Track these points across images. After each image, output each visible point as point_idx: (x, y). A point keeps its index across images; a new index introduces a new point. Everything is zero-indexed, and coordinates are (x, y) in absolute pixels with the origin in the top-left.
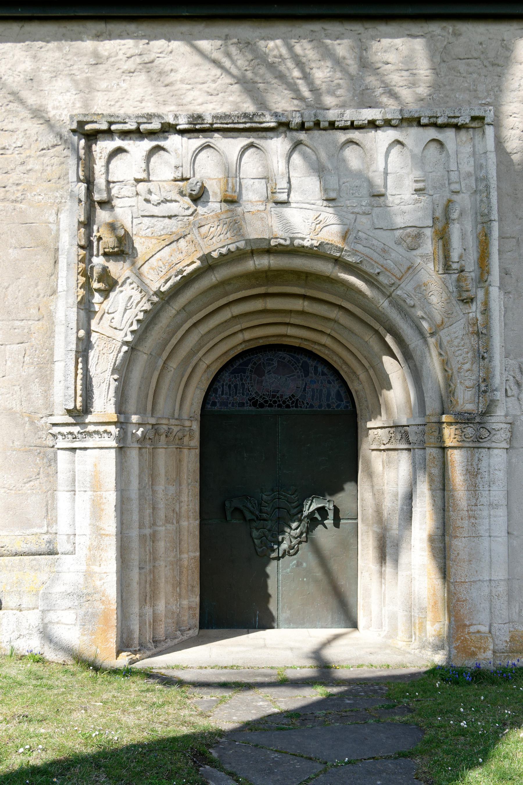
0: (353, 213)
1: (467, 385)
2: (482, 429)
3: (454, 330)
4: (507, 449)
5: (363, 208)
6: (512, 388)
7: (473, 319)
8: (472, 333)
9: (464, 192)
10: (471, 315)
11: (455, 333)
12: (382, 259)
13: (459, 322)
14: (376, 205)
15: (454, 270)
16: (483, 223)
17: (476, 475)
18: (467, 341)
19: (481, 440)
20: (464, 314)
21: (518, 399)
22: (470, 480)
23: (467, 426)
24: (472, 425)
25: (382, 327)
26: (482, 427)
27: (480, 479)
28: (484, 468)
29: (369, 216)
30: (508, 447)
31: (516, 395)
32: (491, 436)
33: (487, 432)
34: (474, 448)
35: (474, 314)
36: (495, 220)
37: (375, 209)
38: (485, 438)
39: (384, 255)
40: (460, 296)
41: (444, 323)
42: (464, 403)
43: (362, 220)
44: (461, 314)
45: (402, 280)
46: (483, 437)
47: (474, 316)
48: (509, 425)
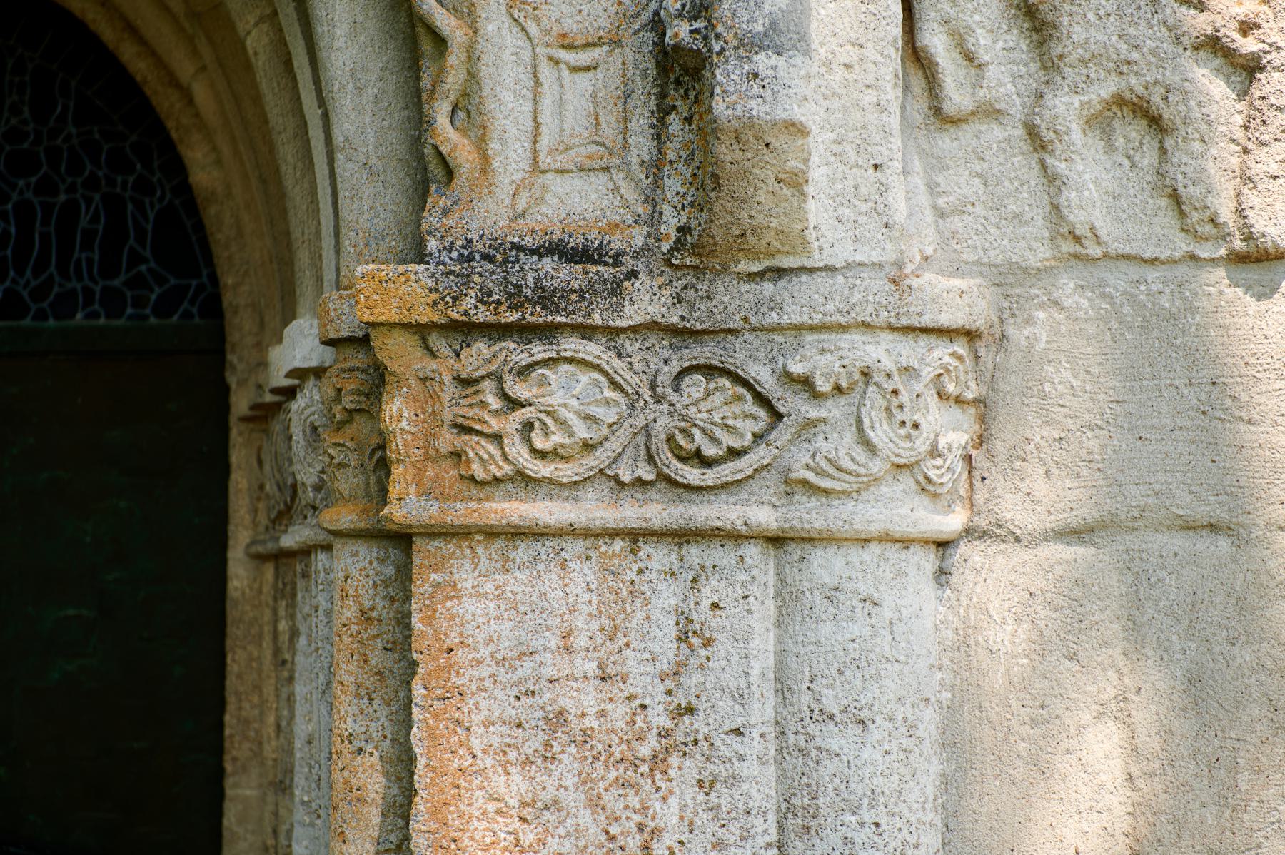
1: (570, 24)
2: (695, 386)
4: (943, 545)
6: (982, 42)
17: (660, 761)
19: (692, 475)
21: (1032, 132)
22: (595, 804)
23: (539, 351)
24: (591, 350)
26: (709, 370)
27: (692, 795)
28: (725, 703)
30: (953, 522)
31: (1017, 109)
32: (782, 435)
33: (750, 406)
34: (635, 536)
38: (734, 453)
42: (536, 168)
46: (710, 451)
48: (960, 348)
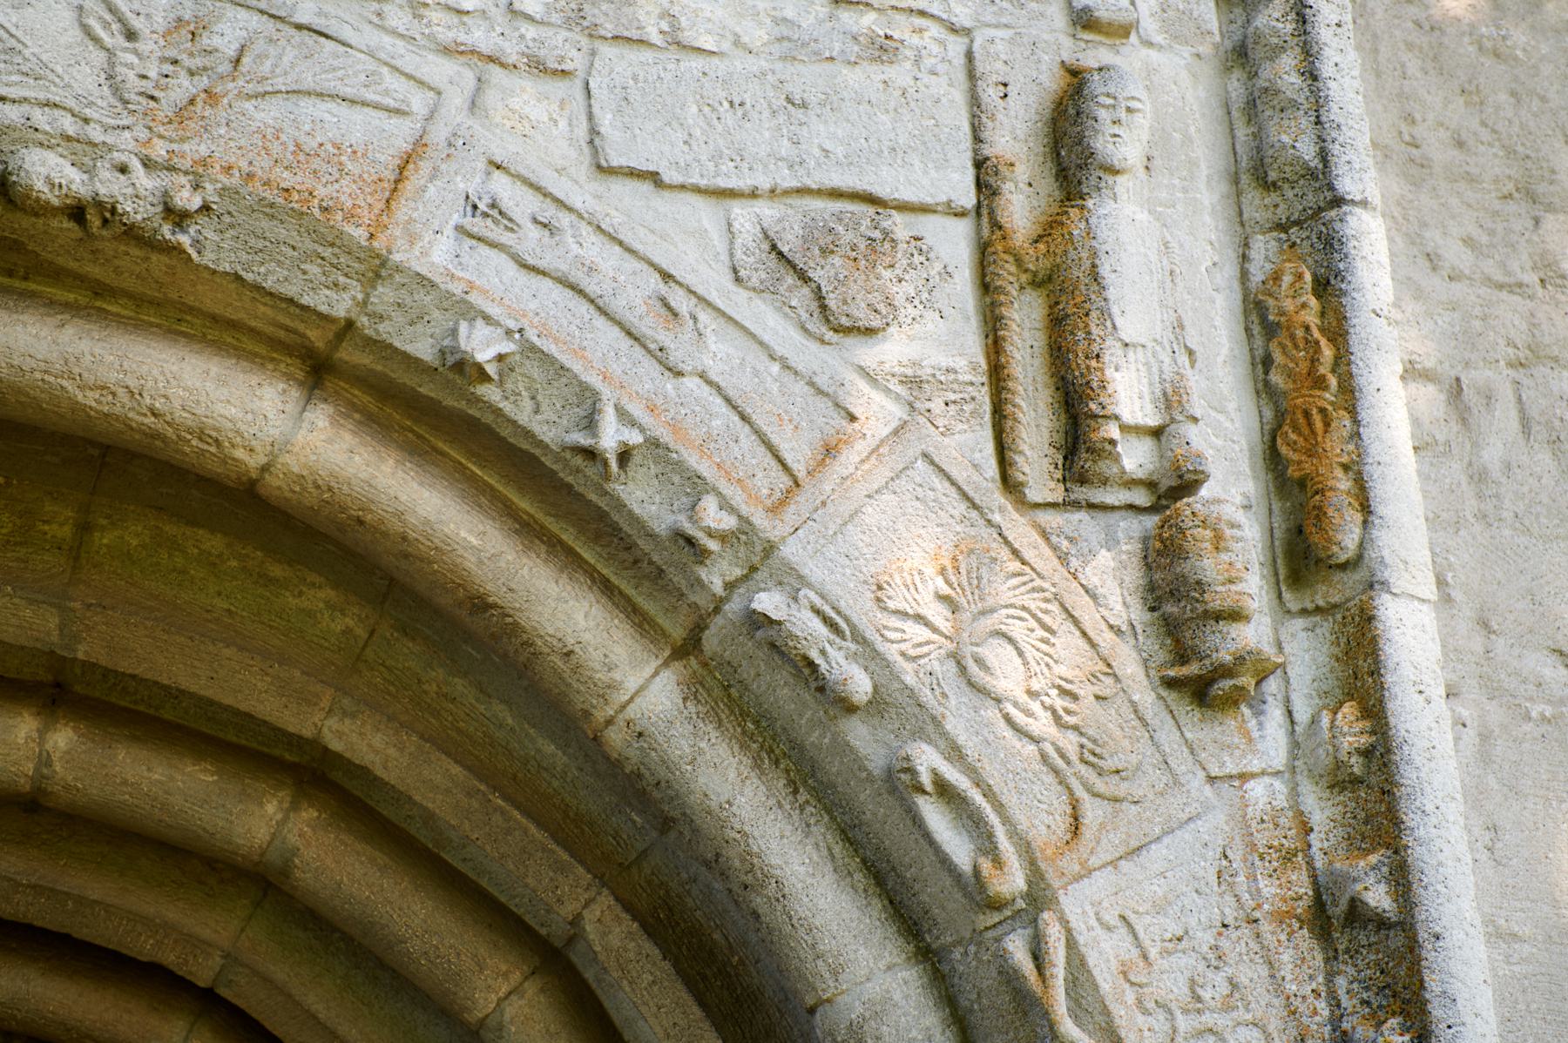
0: (450, 51)
3: (1158, 889)
5: (530, 31)
7: (1272, 818)
8: (1280, 918)
9: (1159, 39)
10: (1257, 790)
11: (1159, 908)
12: (650, 367)
13: (1186, 835)
14: (608, 29)
15: (1131, 483)
16: (1282, 227)
18: (1251, 974)
20: (1212, 779)
25: (606, 900)
29: (558, 88)
35: (1278, 785)
36: (1364, 203)
37: (607, 51)
39: (664, 338)
40: (1182, 658)
41: (1088, 833)
43: (515, 103)
44: (1197, 781)
45: (791, 515)
47: (1281, 801)
